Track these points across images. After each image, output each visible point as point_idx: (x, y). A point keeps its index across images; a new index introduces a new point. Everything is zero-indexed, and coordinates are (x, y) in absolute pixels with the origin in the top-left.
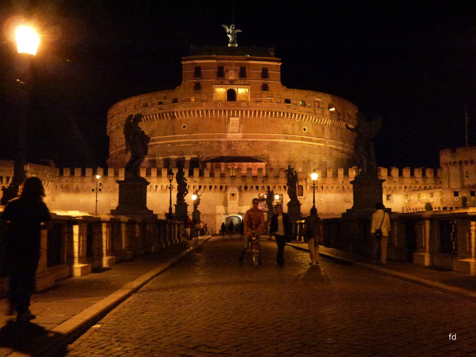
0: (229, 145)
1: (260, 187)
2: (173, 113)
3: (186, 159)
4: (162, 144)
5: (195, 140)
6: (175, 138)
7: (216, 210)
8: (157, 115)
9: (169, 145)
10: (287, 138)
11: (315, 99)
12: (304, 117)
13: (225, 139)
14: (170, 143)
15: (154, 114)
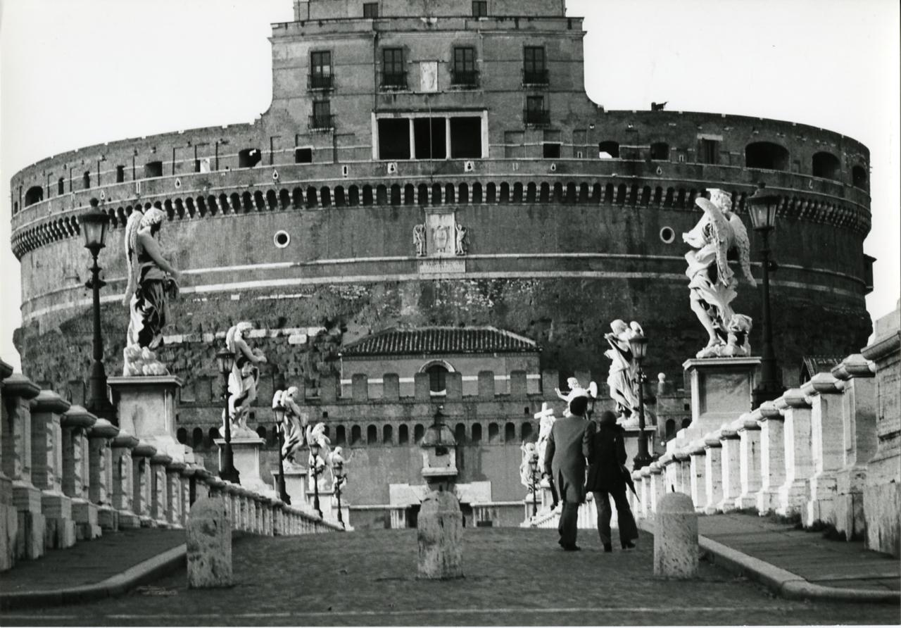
0: (427, 291)
1: (518, 425)
2: (247, 195)
3: (292, 340)
4: (210, 295)
5: (316, 281)
6: (251, 275)
7: (386, 497)
8: (195, 203)
9: (235, 297)
10: (609, 265)
11: (700, 137)
12: (665, 193)
13: (413, 277)
14: (236, 292)
15: (184, 199)
